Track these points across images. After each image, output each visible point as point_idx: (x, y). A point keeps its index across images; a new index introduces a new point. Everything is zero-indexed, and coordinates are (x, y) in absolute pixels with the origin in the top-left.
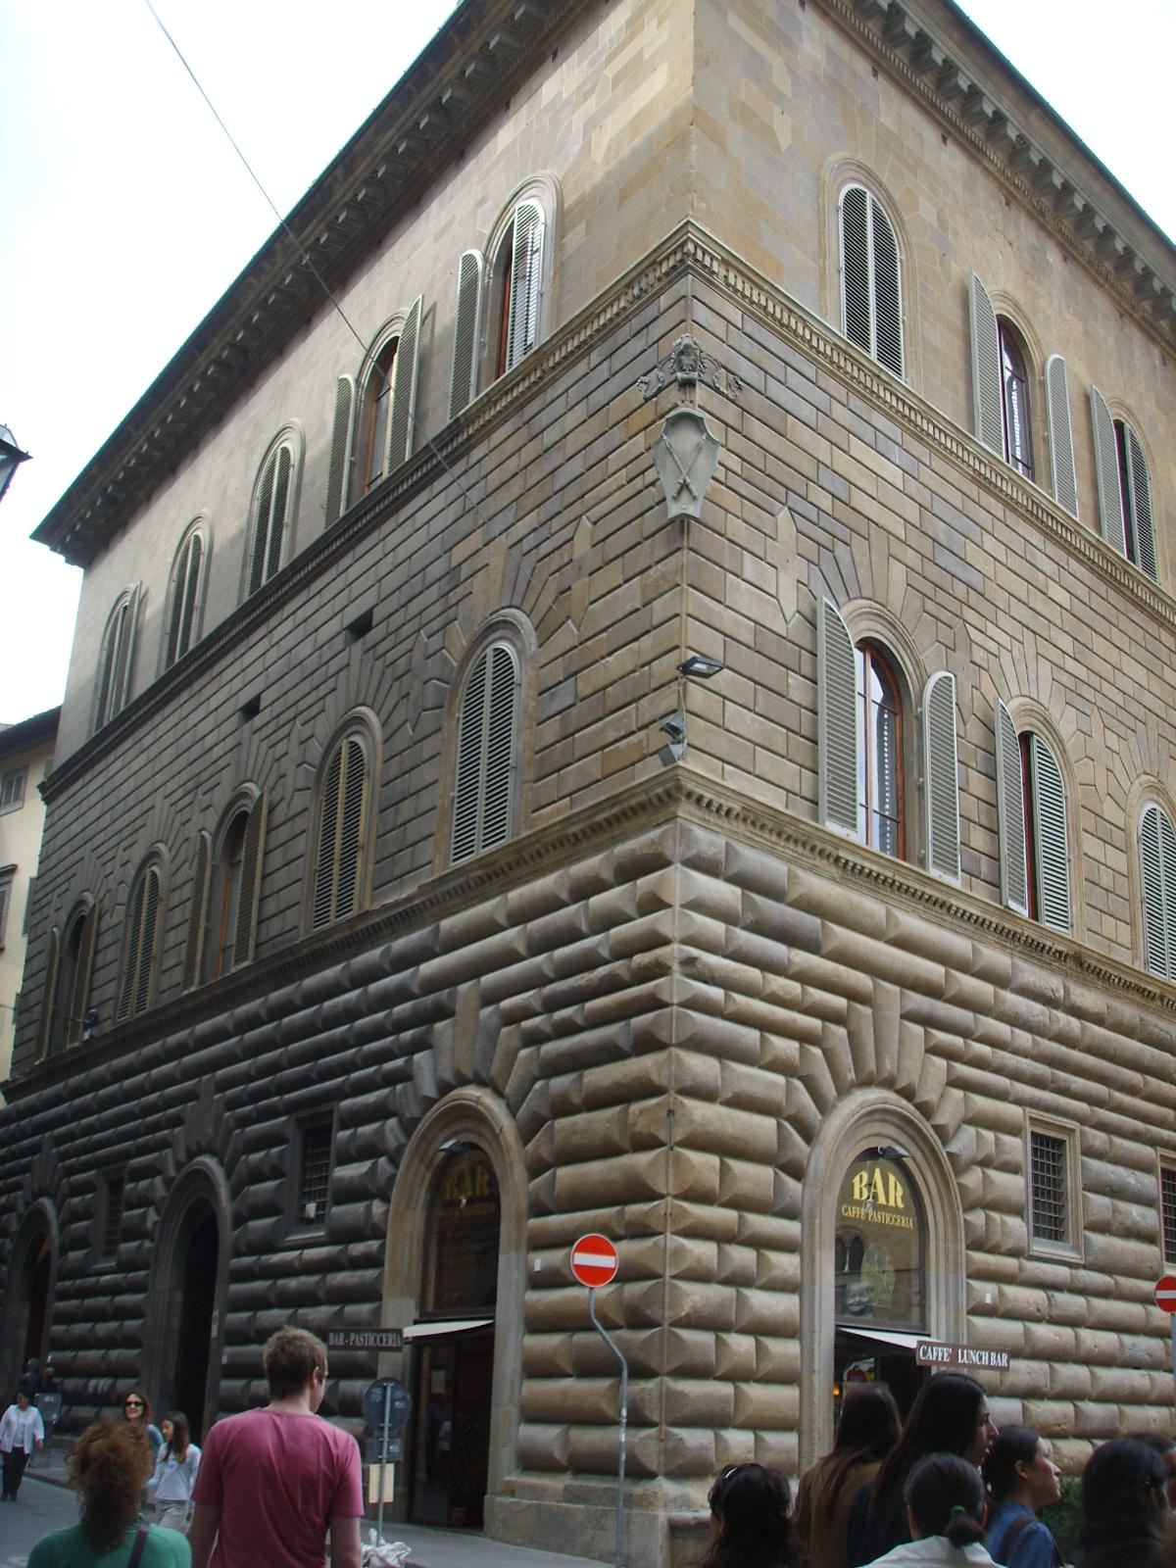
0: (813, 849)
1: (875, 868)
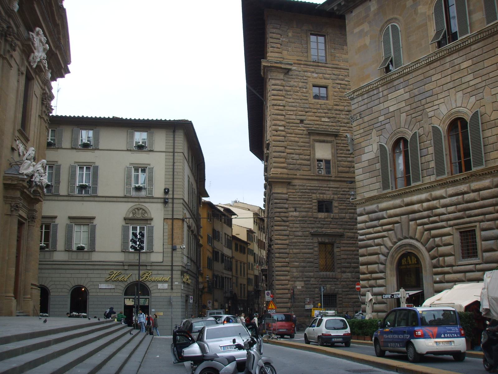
0: (382, 198)
1: (396, 193)
